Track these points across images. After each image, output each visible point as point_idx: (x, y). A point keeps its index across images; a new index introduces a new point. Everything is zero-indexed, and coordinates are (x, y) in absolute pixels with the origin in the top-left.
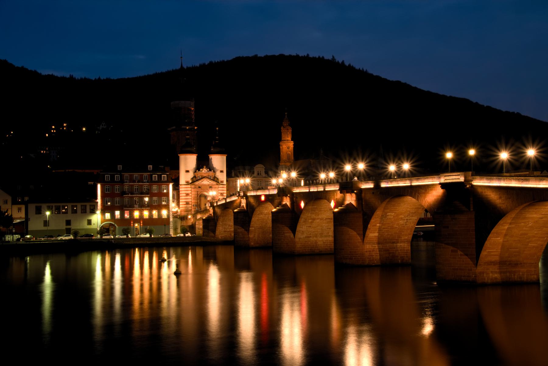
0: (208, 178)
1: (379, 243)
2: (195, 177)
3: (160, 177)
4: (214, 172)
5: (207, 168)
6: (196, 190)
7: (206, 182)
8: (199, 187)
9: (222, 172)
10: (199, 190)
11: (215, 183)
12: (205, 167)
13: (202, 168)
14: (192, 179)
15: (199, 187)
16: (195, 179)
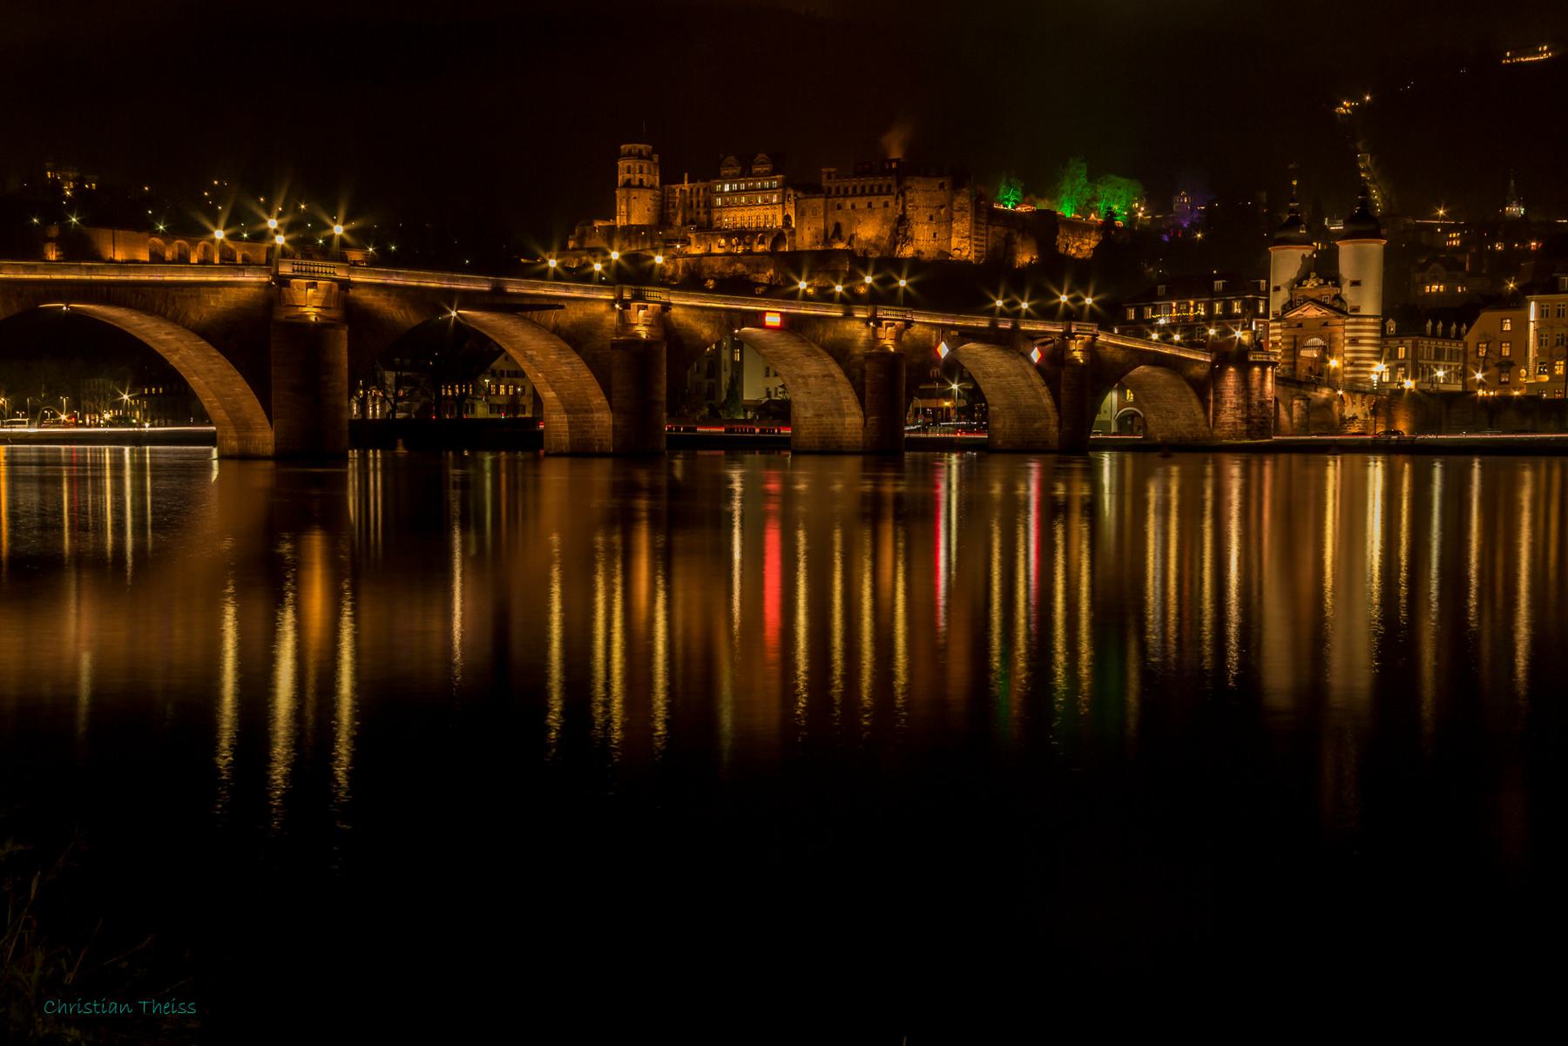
0: (1319, 303)
1: (567, 412)
2: (1291, 302)
3: (1227, 307)
4: (1337, 284)
5: (1319, 276)
6: (1291, 332)
7: (1312, 312)
8: (1300, 325)
9: (1356, 283)
10: (1298, 332)
11: (1331, 314)
12: (1313, 274)
13: (1307, 277)
14: (1284, 307)
15: (1300, 325)
16: (1290, 305)
